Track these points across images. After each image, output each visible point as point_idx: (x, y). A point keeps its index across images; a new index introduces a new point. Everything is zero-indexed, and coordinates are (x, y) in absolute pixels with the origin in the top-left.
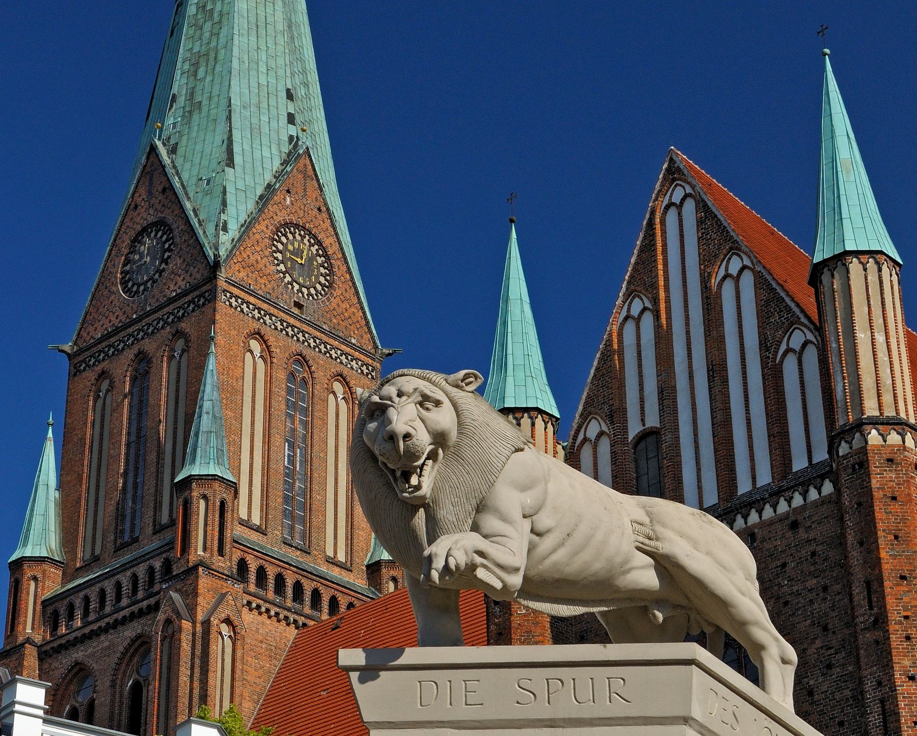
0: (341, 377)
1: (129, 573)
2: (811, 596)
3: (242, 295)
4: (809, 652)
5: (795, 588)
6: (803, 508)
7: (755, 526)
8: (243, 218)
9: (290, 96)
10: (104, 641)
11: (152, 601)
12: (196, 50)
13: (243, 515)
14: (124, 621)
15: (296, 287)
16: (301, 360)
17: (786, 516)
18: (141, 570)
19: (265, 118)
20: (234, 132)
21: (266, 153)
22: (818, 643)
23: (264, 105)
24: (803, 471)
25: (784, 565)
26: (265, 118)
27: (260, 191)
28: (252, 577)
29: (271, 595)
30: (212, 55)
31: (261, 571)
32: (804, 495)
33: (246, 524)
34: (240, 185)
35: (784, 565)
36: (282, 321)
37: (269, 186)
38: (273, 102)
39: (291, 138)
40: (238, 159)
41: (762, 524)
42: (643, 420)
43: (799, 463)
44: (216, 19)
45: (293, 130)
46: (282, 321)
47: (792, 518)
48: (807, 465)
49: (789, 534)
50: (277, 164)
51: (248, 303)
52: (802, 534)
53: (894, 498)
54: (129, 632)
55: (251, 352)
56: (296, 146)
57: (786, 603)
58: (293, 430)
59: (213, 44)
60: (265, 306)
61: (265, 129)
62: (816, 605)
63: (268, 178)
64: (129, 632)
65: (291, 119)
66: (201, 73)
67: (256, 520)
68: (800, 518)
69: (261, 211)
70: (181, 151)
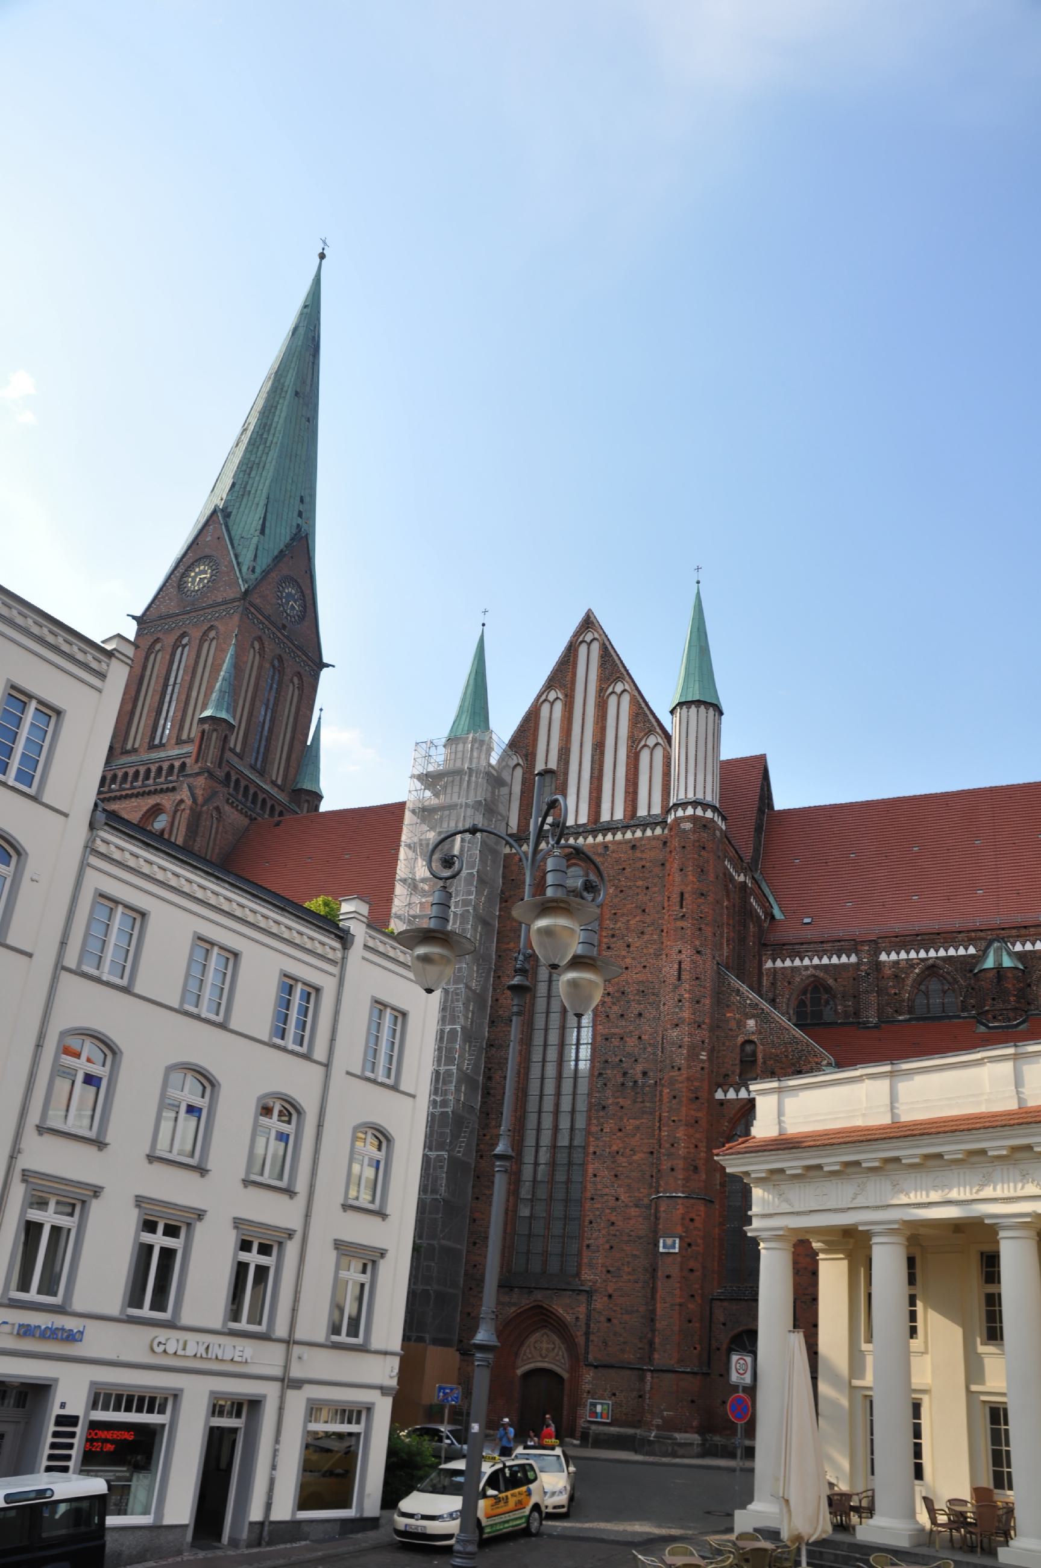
0: (299, 675)
1: (157, 765)
2: (639, 890)
3: (255, 612)
4: (631, 922)
5: (628, 884)
6: (641, 839)
7: (610, 842)
8: (264, 567)
9: (302, 501)
10: (134, 802)
11: (170, 785)
12: (252, 459)
13: (232, 746)
14: (149, 793)
15: (285, 615)
16: (280, 659)
17: (630, 841)
18: (165, 766)
19: (286, 510)
20: (268, 514)
21: (283, 531)
22: (638, 918)
23: (287, 502)
24: (644, 817)
25: (624, 869)
26: (286, 510)
27: (276, 553)
28: (232, 785)
29: (240, 797)
30: (262, 464)
31: (237, 782)
32: (644, 831)
33: (232, 751)
34: (266, 547)
35: (624, 869)
36: (274, 633)
37: (281, 551)
38: (292, 501)
39: (298, 525)
40: (267, 531)
41: (614, 842)
42: (546, 763)
43: (642, 812)
44: (268, 445)
45: (300, 521)
46: (274, 633)
47: (633, 843)
48: (646, 814)
49: (630, 852)
50: (288, 538)
51: (258, 618)
52: (638, 854)
53: (704, 848)
54: (151, 801)
55: (254, 648)
56: (300, 530)
57: (622, 891)
58: (268, 700)
59: (264, 459)
60: (266, 622)
61: (285, 517)
62: (640, 896)
63: (282, 546)
64: (151, 801)
65: (300, 514)
66: (253, 474)
67: (238, 750)
68: (638, 844)
69: (275, 565)
70: (232, 517)
